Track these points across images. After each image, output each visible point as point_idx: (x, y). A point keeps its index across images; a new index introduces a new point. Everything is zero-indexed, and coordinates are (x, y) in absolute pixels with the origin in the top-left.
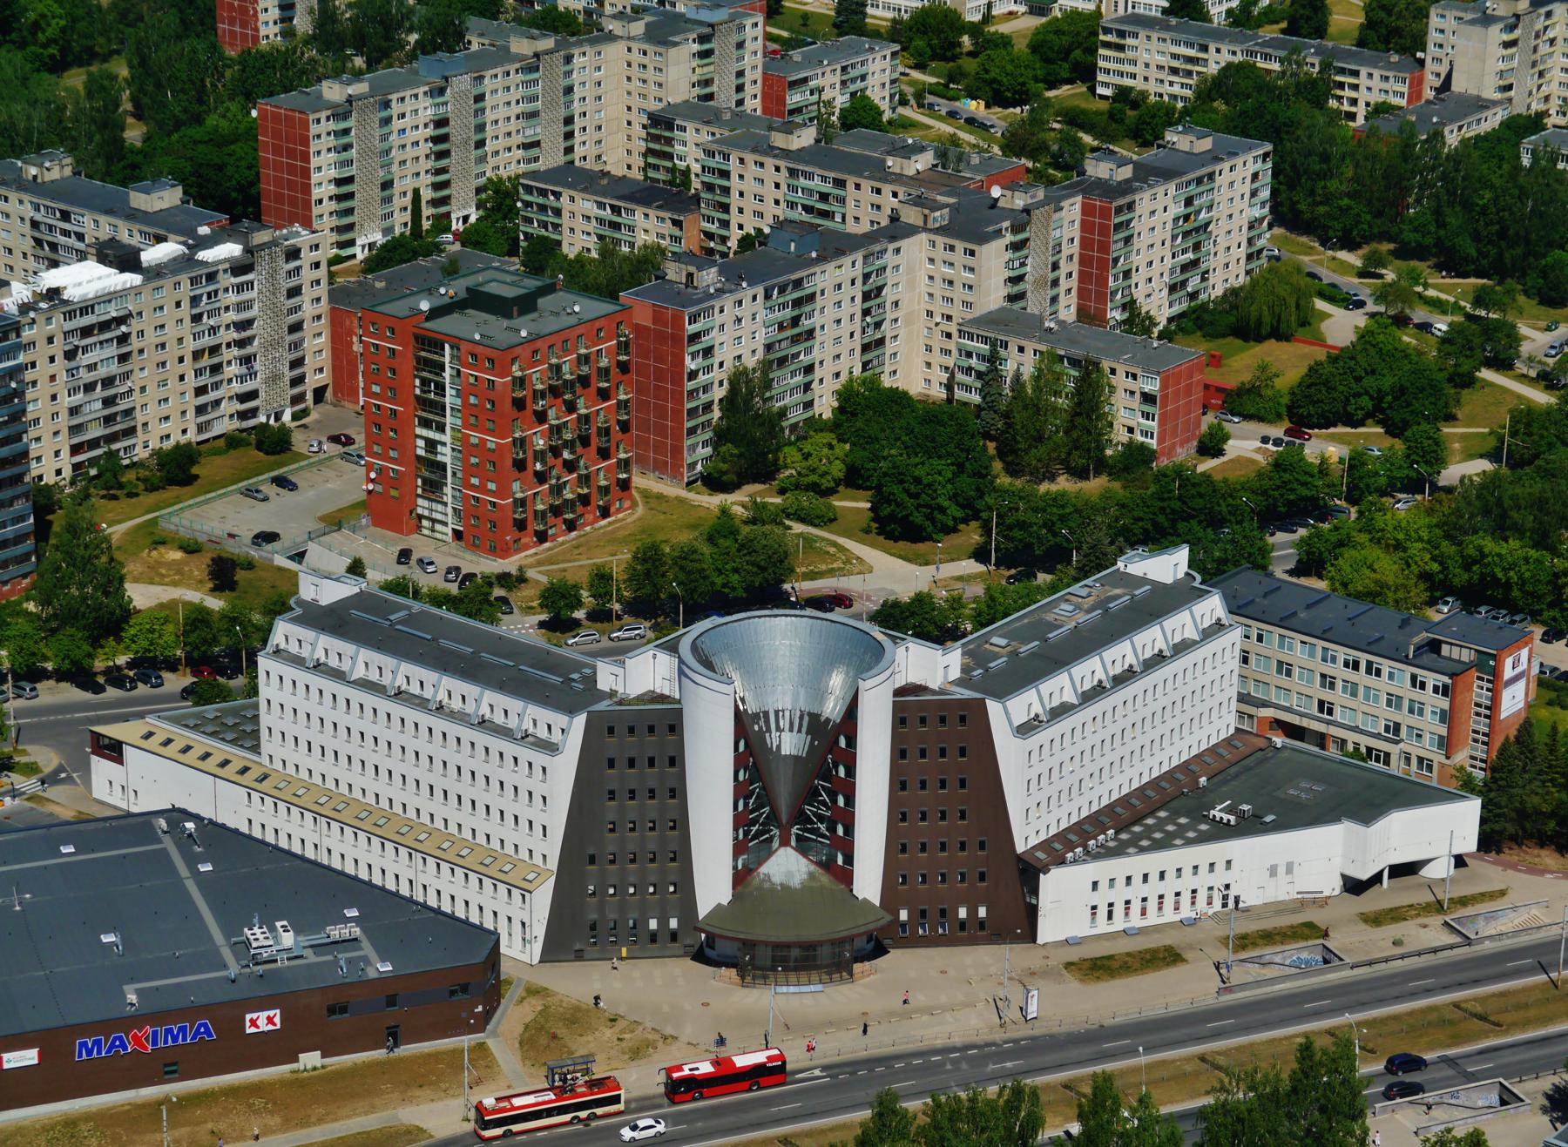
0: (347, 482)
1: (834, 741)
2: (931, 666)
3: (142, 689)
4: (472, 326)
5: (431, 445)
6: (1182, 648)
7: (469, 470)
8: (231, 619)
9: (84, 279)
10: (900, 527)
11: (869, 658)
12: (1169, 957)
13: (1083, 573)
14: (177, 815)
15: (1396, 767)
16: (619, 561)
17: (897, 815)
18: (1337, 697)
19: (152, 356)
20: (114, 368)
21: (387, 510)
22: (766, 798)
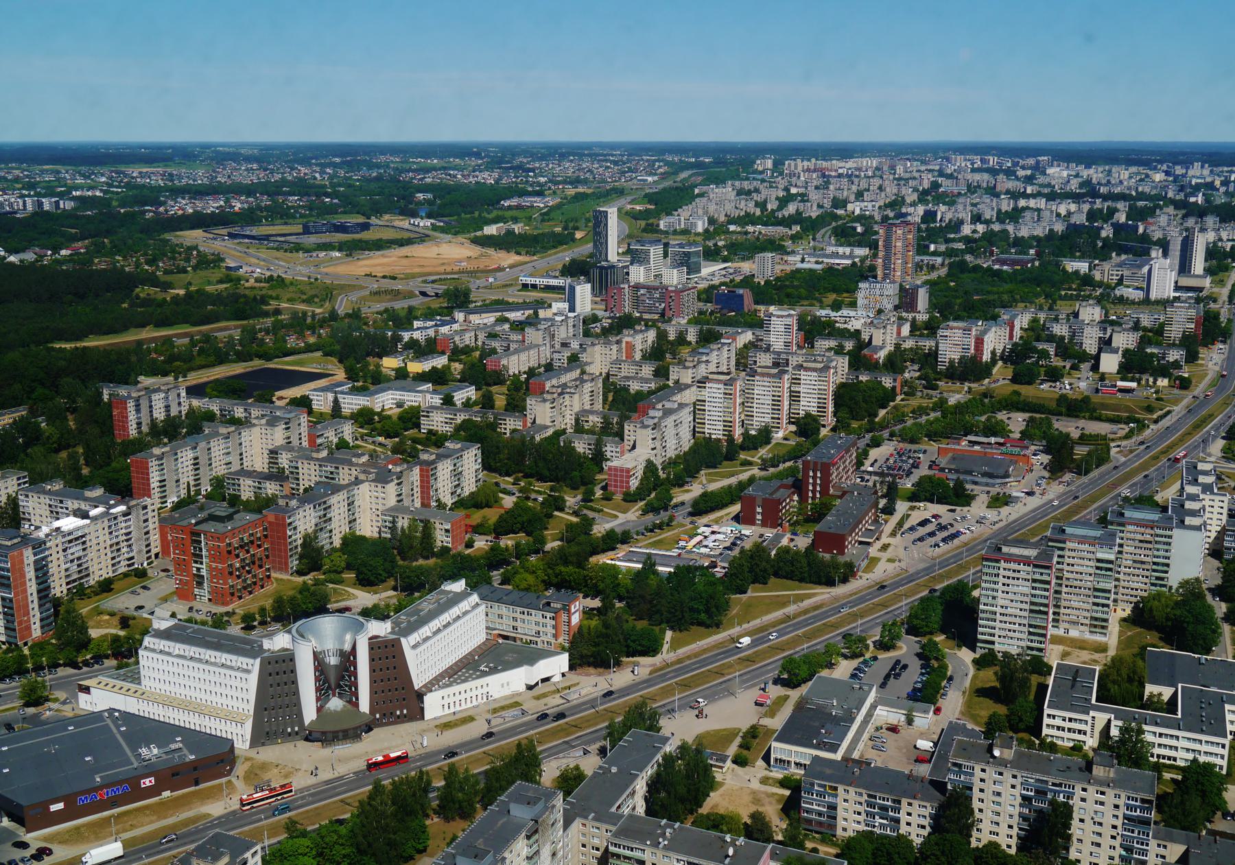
0: (170, 585)
1: (348, 658)
2: (380, 629)
3: (96, 666)
4: (211, 527)
5: (198, 569)
6: (466, 613)
7: (213, 577)
8: (128, 638)
9: (69, 523)
10: (366, 582)
11: (360, 627)
12: (471, 719)
13: (430, 591)
14: (111, 711)
15: (540, 646)
16: (268, 603)
17: (373, 682)
18: (518, 624)
19: (95, 548)
20: (81, 553)
21: (183, 593)
22: (326, 681)
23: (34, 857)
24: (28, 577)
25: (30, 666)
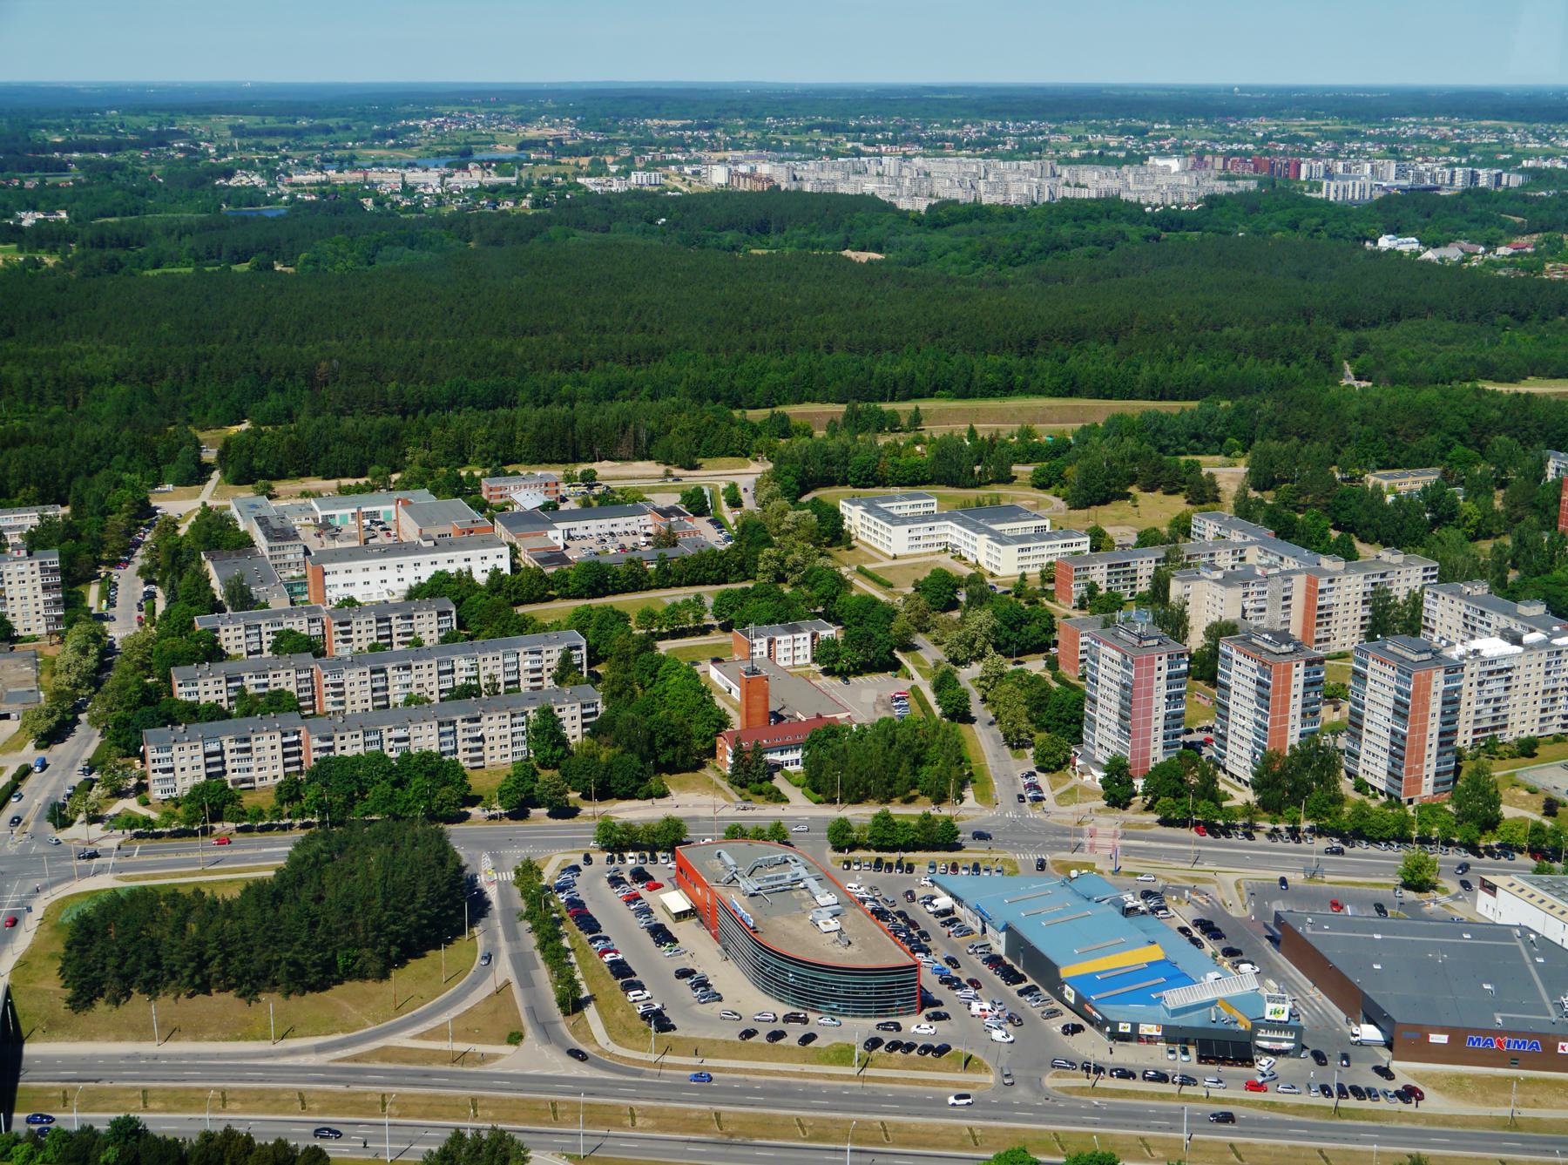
3: (1503, 860)
8: (1558, 833)
9: (1493, 646)
20: (1501, 693)
23: (1398, 1094)
24: (1431, 711)
25: (1415, 834)
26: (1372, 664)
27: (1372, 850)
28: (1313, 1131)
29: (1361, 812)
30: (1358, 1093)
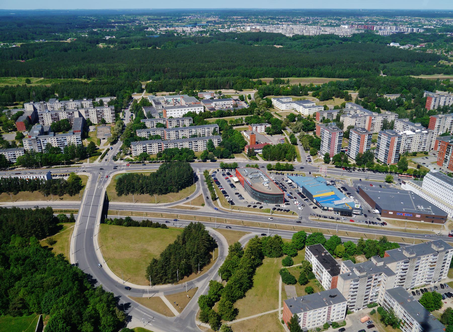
0: (436, 159)
5: (447, 157)
7: (451, 161)
8: (420, 172)
9: (409, 132)
14: (411, 192)
19: (414, 142)
20: (410, 142)
21: (439, 163)
23: (381, 223)
25: (389, 171)
26: (382, 135)
27: (380, 174)
28: (363, 230)
29: (378, 166)
30: (373, 223)
